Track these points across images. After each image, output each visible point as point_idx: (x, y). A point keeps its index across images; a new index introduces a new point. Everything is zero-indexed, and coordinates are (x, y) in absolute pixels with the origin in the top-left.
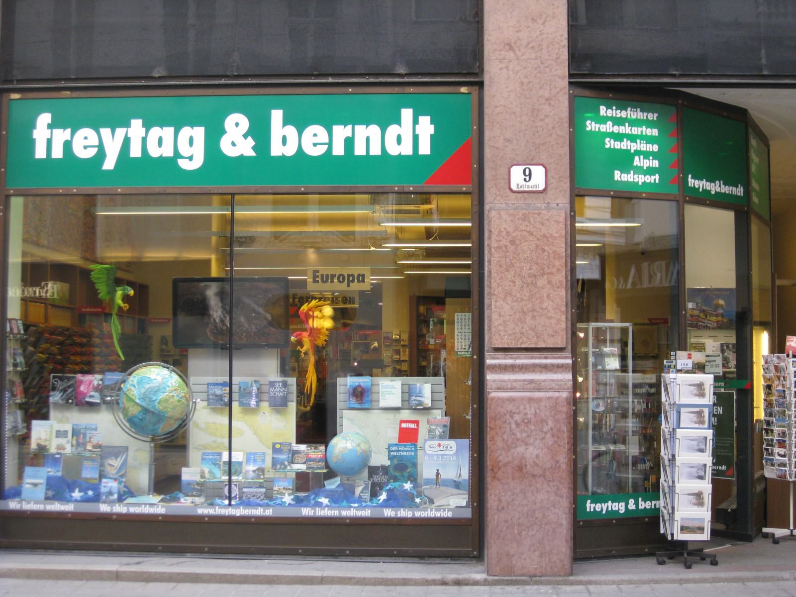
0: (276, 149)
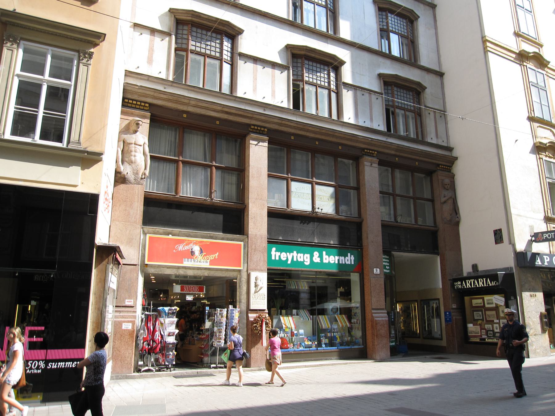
0: (325, 261)
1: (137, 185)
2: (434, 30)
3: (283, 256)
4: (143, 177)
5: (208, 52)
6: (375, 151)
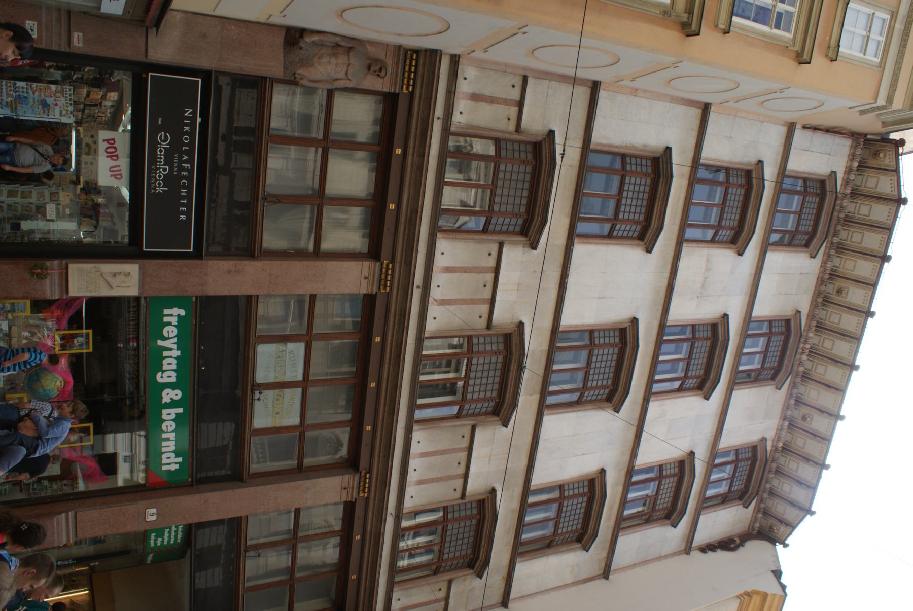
0: (165, 412)
2: (571, 581)
3: (171, 331)
4: (296, 75)
5: (499, 191)
6: (369, 492)
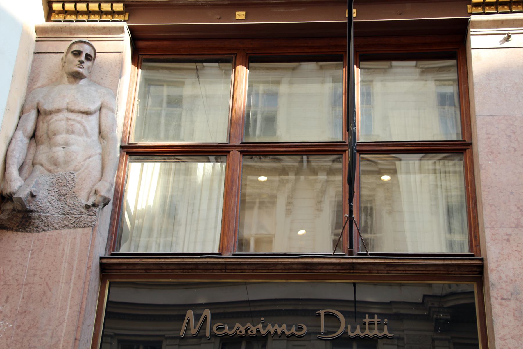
1: (72, 230)
4: (90, 203)
